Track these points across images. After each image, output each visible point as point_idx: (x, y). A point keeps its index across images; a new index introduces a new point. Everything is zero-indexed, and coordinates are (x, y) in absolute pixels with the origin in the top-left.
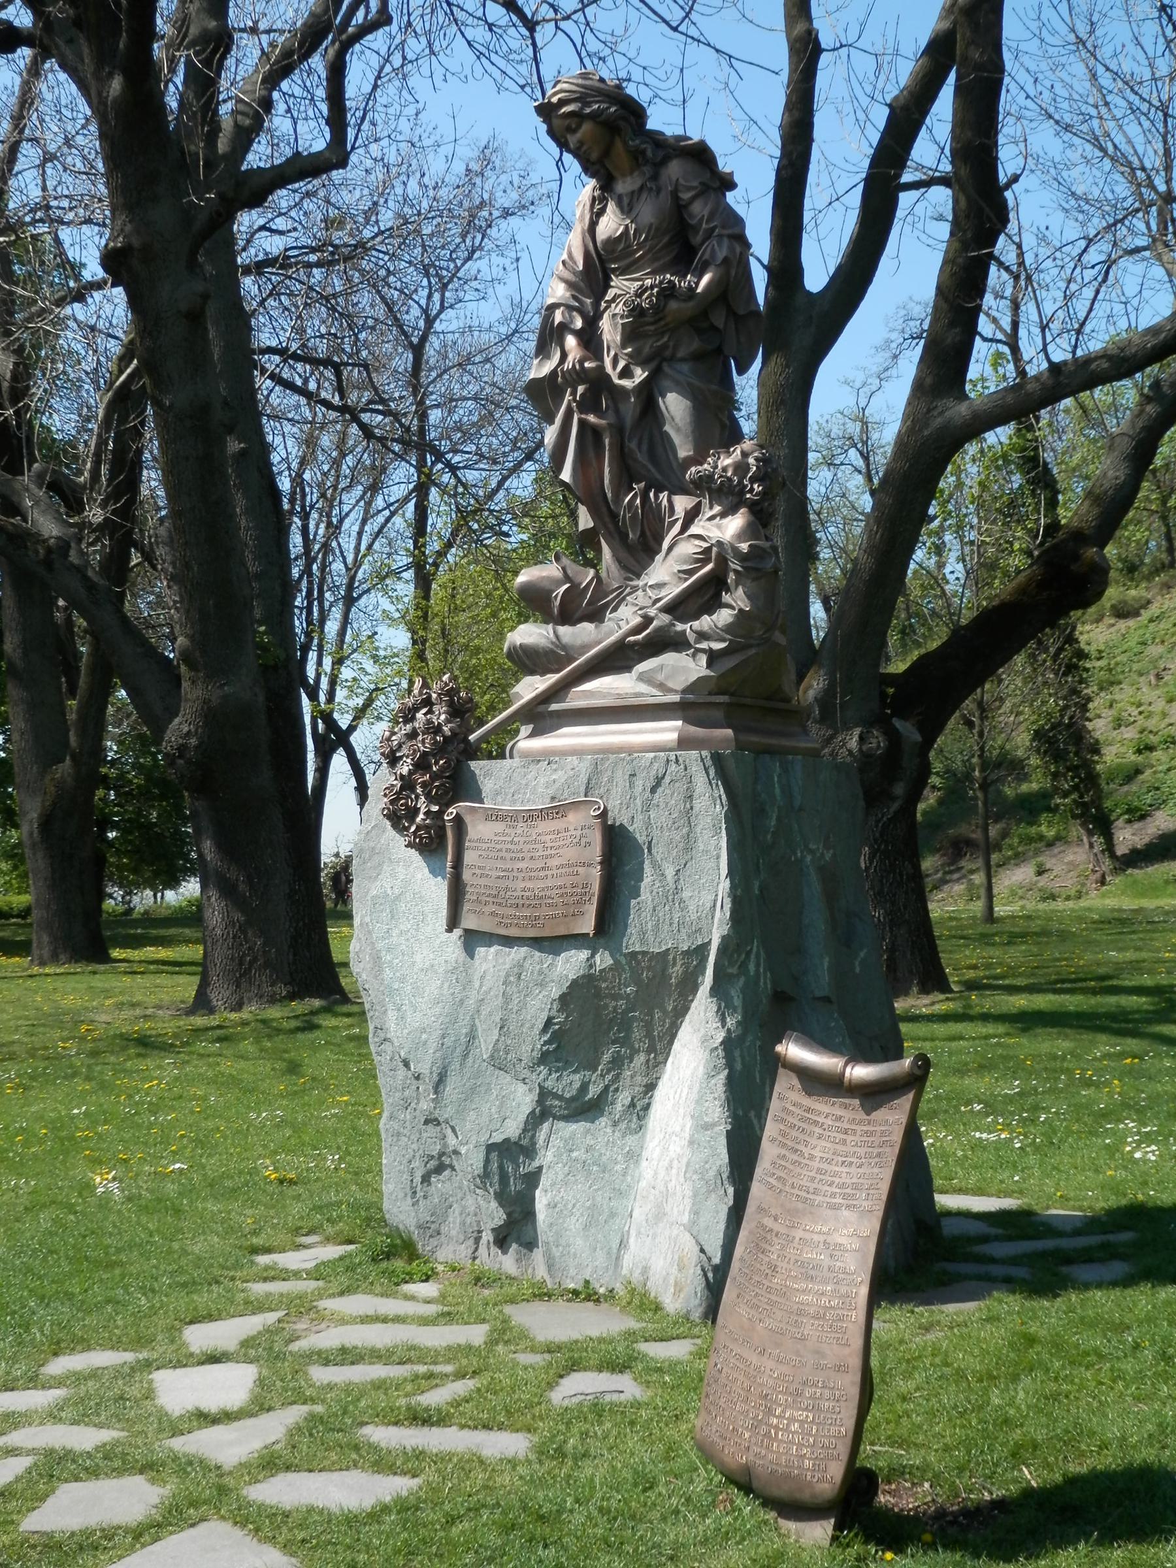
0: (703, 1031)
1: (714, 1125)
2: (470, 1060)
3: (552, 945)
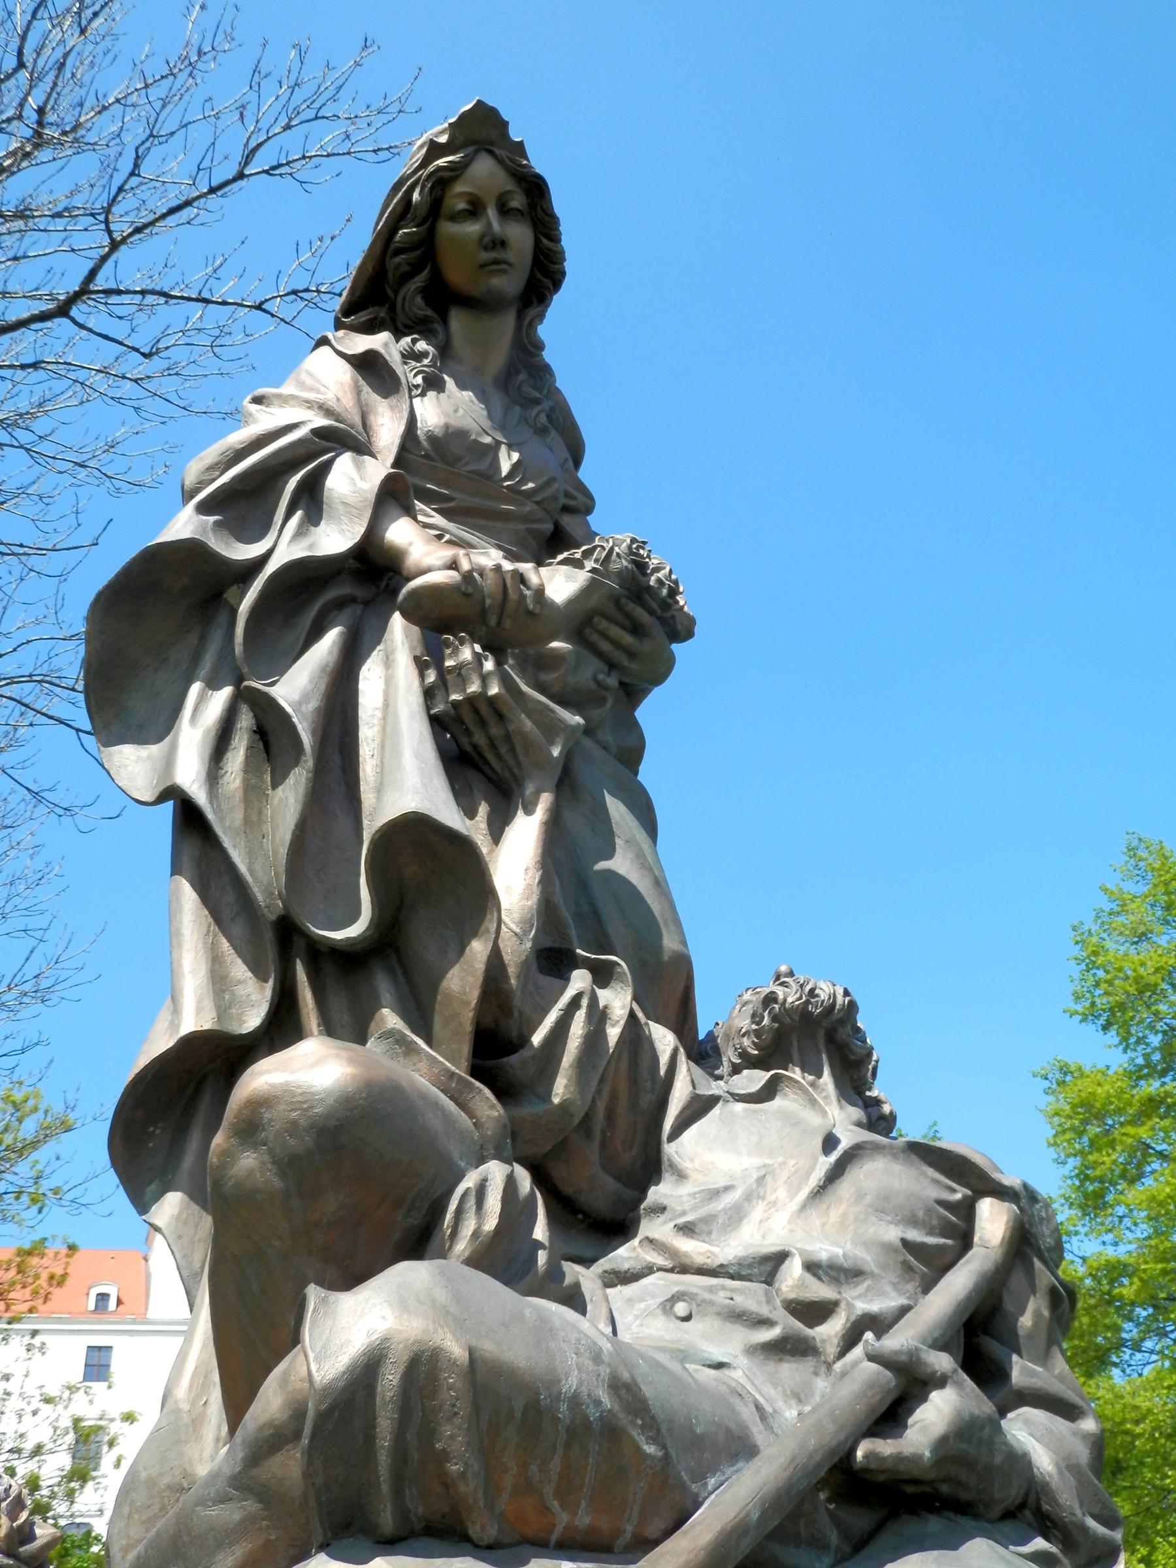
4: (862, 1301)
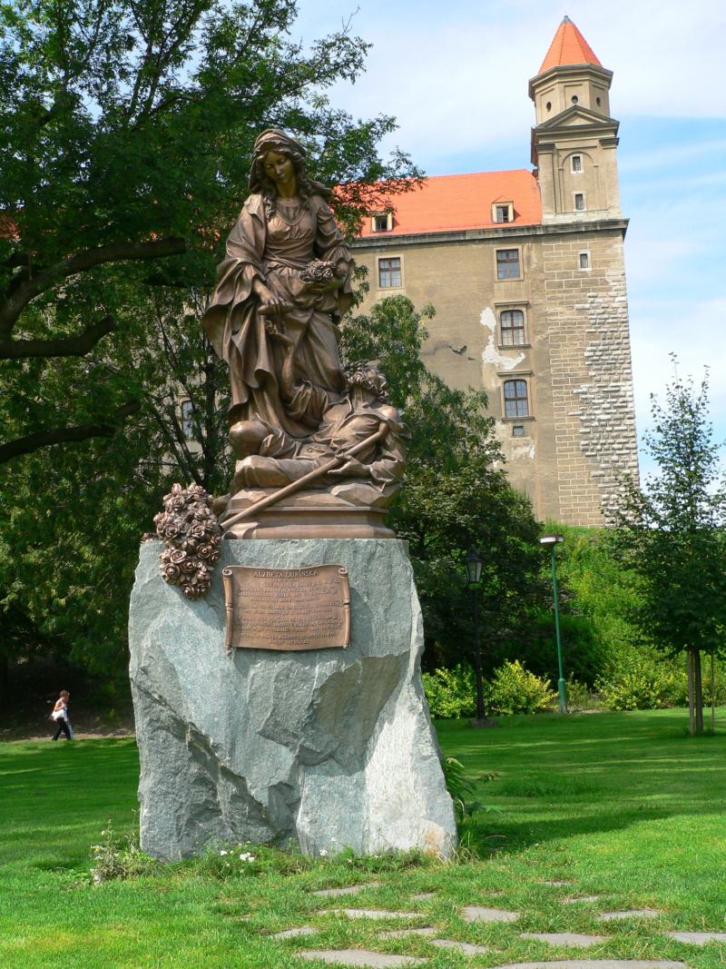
0: (409, 704)
1: (429, 757)
2: (248, 733)
3: (309, 653)
4: (344, 446)
